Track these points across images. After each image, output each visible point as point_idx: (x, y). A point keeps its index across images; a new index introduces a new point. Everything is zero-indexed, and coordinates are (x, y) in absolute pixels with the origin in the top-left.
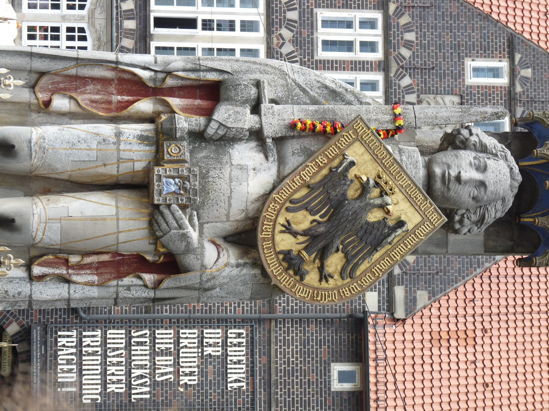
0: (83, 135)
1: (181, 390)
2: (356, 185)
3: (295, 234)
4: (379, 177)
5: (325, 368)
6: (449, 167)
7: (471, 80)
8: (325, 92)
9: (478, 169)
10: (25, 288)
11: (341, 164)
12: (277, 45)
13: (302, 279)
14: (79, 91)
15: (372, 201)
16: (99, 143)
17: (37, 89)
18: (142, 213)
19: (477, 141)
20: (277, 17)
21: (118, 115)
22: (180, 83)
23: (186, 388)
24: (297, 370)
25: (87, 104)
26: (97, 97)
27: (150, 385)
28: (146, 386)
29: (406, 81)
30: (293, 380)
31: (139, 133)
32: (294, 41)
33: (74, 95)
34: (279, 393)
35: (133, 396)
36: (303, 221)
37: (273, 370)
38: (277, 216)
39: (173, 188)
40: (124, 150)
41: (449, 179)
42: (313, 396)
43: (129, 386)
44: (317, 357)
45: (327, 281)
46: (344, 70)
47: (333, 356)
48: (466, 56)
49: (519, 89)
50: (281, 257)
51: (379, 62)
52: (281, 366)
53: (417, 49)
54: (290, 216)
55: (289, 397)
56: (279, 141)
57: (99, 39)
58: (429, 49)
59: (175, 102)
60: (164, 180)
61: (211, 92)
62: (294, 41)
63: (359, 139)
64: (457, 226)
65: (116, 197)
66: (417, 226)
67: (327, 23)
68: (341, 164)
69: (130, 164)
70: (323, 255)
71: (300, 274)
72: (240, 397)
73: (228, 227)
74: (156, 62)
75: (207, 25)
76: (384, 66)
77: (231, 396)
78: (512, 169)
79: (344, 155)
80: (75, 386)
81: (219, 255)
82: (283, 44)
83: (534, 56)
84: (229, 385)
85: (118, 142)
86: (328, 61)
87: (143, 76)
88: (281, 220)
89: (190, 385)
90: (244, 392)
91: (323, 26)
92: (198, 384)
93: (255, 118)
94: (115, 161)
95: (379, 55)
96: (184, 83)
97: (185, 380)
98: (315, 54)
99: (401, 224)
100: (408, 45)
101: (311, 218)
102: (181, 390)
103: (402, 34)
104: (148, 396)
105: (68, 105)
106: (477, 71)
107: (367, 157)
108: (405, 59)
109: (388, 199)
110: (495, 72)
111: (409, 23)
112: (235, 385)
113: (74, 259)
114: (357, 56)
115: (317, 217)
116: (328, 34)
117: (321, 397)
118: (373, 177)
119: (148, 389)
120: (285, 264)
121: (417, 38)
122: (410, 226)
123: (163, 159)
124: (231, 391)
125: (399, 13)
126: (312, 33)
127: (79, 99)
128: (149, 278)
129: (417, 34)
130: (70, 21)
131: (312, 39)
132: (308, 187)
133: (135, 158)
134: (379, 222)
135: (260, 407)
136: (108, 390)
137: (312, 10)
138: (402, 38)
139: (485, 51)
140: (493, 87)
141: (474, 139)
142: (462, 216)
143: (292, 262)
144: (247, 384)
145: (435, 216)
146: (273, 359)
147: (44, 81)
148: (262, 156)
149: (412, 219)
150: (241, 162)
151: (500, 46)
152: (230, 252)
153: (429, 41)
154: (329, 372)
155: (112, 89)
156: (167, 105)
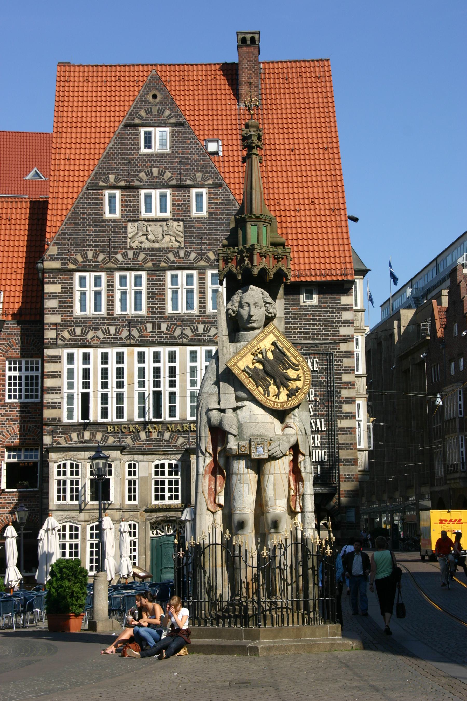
1: (318, 399)
2: (257, 365)
3: (279, 393)
5: (303, 309)
7: (117, 215)
10: (307, 514)
11: (247, 373)
12: (98, 341)
13: (300, 389)
16: (240, 483)
20: (80, 341)
23: (318, 396)
24: (305, 326)
27: (316, 419)
28: (316, 422)
29: (119, 257)
30: (312, 329)
32: (96, 330)
34: (320, 338)
35: (323, 429)
36: (273, 389)
37: (306, 342)
38: (272, 401)
42: (321, 316)
43: (317, 431)
44: (297, 314)
46: (113, 297)
47: (296, 304)
48: (102, 218)
49: (123, 183)
50: (290, 399)
51: (107, 274)
52: (302, 337)
53: (99, 250)
54: (271, 395)
55: (322, 331)
58: (98, 242)
60: (257, 453)
62: (96, 330)
63: (236, 364)
64: (273, 315)
66: (275, 336)
67: (83, 308)
68: (247, 373)
70: (289, 379)
71: (297, 389)
72: (322, 363)
73: (277, 422)
75: (86, 385)
76: (110, 271)
77: (322, 368)
79: (243, 371)
80: (317, 465)
81: (291, 427)
82: (97, 337)
83: (100, 173)
84: (315, 369)
86: (108, 308)
88: (273, 399)
89: (315, 394)
90: (319, 360)
91: (85, 311)
92: (315, 389)
93: (227, 411)
95: (103, 275)
97: (312, 398)
98: (103, 316)
99: (274, 344)
100: (96, 256)
101: (272, 386)
102: (318, 399)
103: (88, 260)
104: (323, 420)
106: (112, 210)
107: (244, 359)
108: (105, 258)
109: (263, 351)
110: (112, 198)
111: (81, 255)
112: (315, 365)
113: (292, 493)
114: (104, 289)
115: (272, 382)
116: (90, 308)
117: (322, 311)
119: (318, 421)
120: (293, 397)
121: (91, 250)
122: (275, 339)
124: (319, 368)
125: (75, 262)
126: (90, 318)
128: (301, 458)
129: (88, 250)
130: (86, 474)
131: (93, 318)
132: (257, 387)
134: (273, 354)
135: (328, 349)
136: (319, 445)
137: (74, 318)
138: (91, 260)
139: (99, 205)
140: (122, 200)
142: (269, 313)
143: (292, 393)
144: (315, 358)
145: (270, 328)
146: (299, 342)
147: (209, 508)
148: (244, 408)
149: (272, 338)
151: (95, 195)
153: (93, 242)
154: (306, 306)
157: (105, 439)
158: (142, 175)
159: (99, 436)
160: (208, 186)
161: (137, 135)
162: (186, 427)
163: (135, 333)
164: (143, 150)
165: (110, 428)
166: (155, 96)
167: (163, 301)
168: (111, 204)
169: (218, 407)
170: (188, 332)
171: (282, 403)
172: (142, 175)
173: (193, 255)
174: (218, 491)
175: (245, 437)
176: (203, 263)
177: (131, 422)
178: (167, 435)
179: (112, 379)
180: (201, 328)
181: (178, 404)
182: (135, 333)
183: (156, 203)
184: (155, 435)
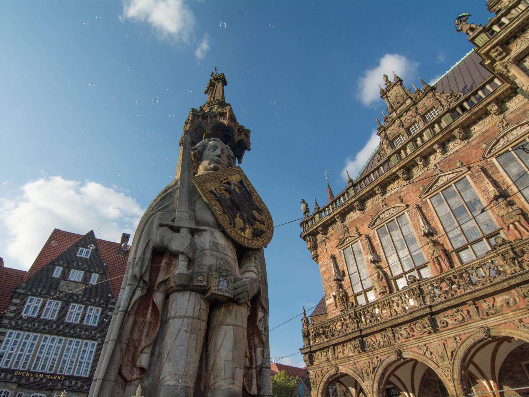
7: (58, 276)
14: (136, 345)
17: (129, 378)
21: (161, 319)
22: (148, 272)
25: (149, 340)
26: (145, 331)
33: (140, 349)
39: (225, 283)
40: (193, 314)
56: (198, 223)
57: (4, 386)
60: (220, 288)
61: (160, 254)
69: (202, 311)
85: (188, 317)
87: (140, 295)
93: (183, 231)
94: (198, 320)
96: (149, 269)
105: (147, 354)
123: (205, 286)
127: (143, 344)
133: (199, 307)
155: (140, 320)
156: (162, 283)
157: (11, 378)
158: (75, 264)
159: (9, 376)
160: (100, 274)
161: (78, 250)
162: (55, 377)
163: (47, 327)
164: (78, 255)
165: (16, 373)
166: (89, 238)
167: (65, 316)
168: (57, 272)
169: (172, 224)
170: (72, 331)
172: (75, 264)
173: (85, 299)
174: (143, 344)
176: (88, 303)
177: (28, 371)
178: (44, 380)
179: (27, 348)
180: (78, 330)
181: (55, 365)
182: (47, 327)
183: (76, 275)
184: (38, 380)
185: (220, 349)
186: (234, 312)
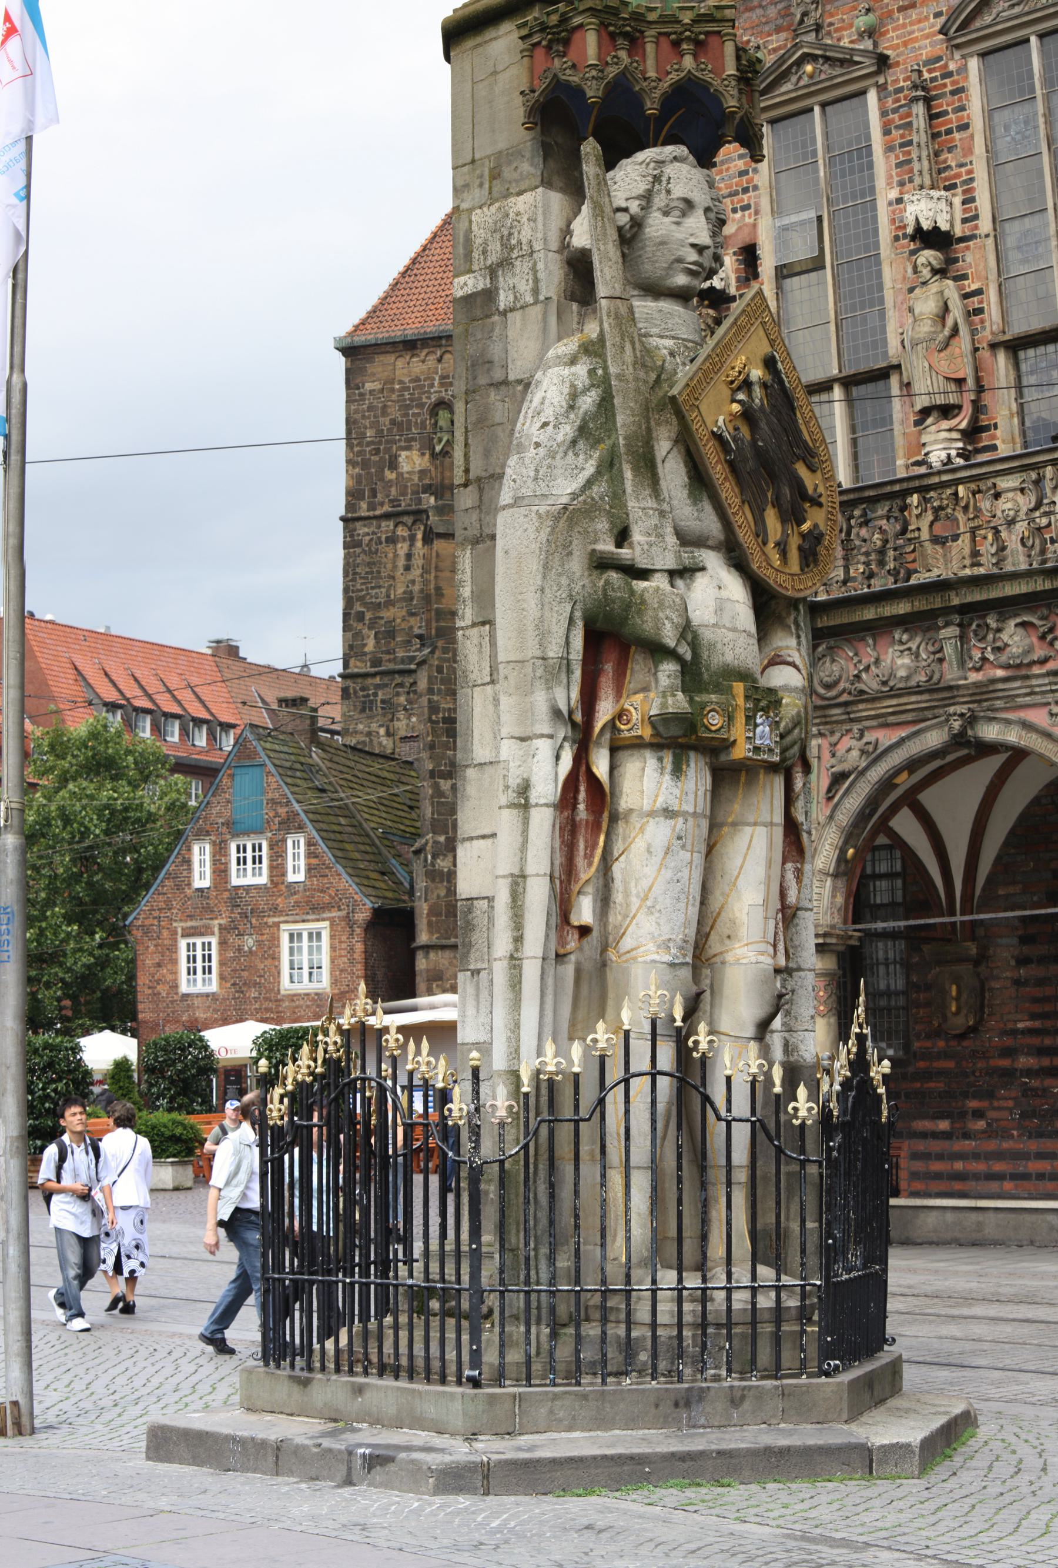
0: (667, 874)
4: (732, 382)
6: (679, 260)
8: (581, 445)
9: (684, 214)
13: (822, 535)
15: (757, 401)
16: (683, 847)
18: (764, 785)
19: (637, 202)
26: (581, 845)
31: (667, 777)
41: (700, 265)
45: (820, 496)
59: (605, 711)
65: (734, 824)
74: (551, 737)
78: (675, 158)
99: (770, 363)
115: (769, 495)
118: (729, 392)
141: (634, 207)
148: (699, 574)
150: (712, 609)
152: (780, 644)
171: (792, 575)
175: (706, 676)
185: (737, 878)
186: (768, 792)
